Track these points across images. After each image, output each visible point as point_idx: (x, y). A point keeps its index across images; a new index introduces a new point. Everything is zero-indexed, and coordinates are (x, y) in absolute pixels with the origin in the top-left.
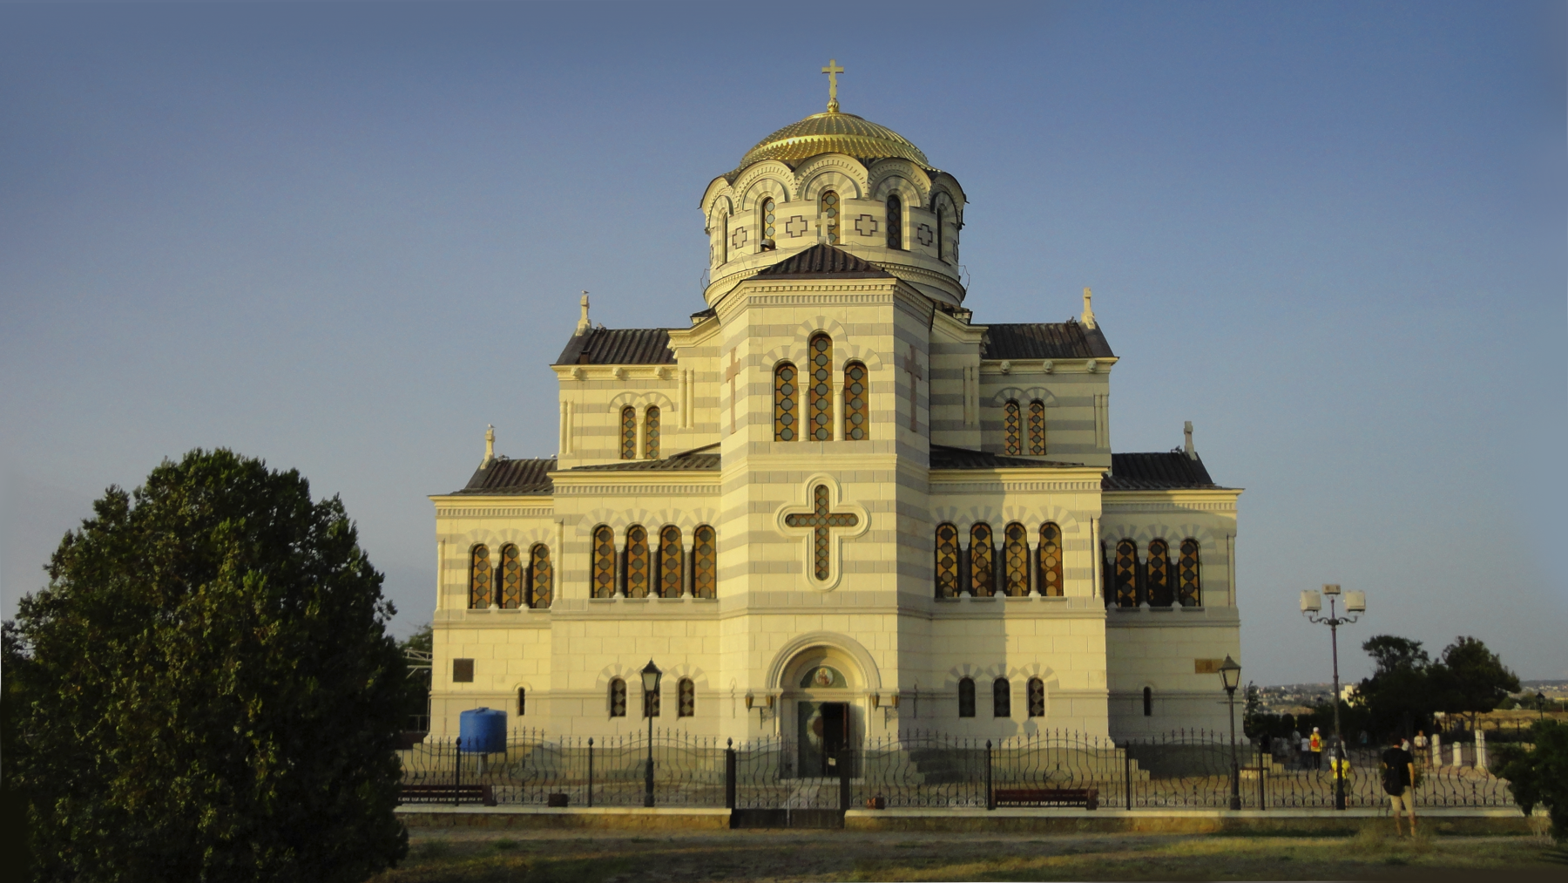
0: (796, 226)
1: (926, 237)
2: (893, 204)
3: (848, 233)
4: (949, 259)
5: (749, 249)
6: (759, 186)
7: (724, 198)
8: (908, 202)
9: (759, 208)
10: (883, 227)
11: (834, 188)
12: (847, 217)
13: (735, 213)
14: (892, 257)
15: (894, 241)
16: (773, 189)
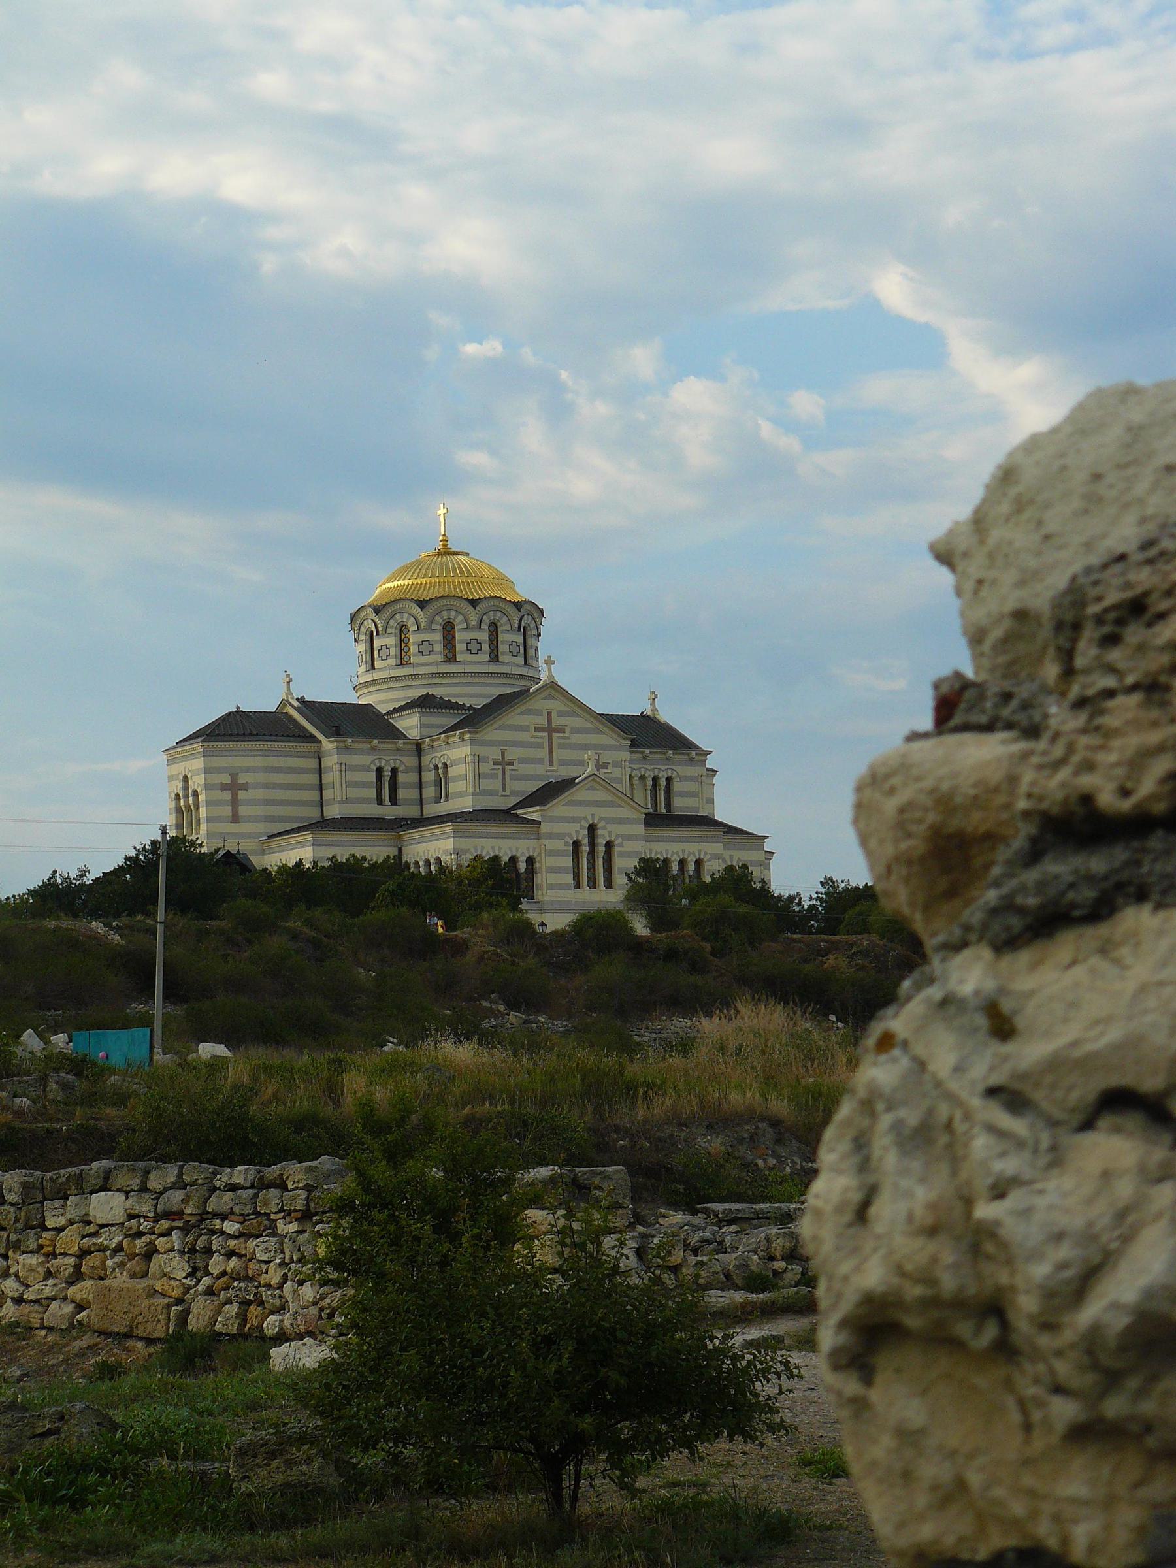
0: (424, 648)
1: (515, 649)
2: (492, 629)
3: (462, 652)
4: (530, 661)
5: (392, 661)
6: (398, 616)
7: (370, 621)
8: (504, 626)
9: (398, 632)
10: (486, 647)
11: (451, 621)
12: (461, 641)
13: (380, 633)
14: (494, 668)
15: (495, 658)
16: (408, 619)
